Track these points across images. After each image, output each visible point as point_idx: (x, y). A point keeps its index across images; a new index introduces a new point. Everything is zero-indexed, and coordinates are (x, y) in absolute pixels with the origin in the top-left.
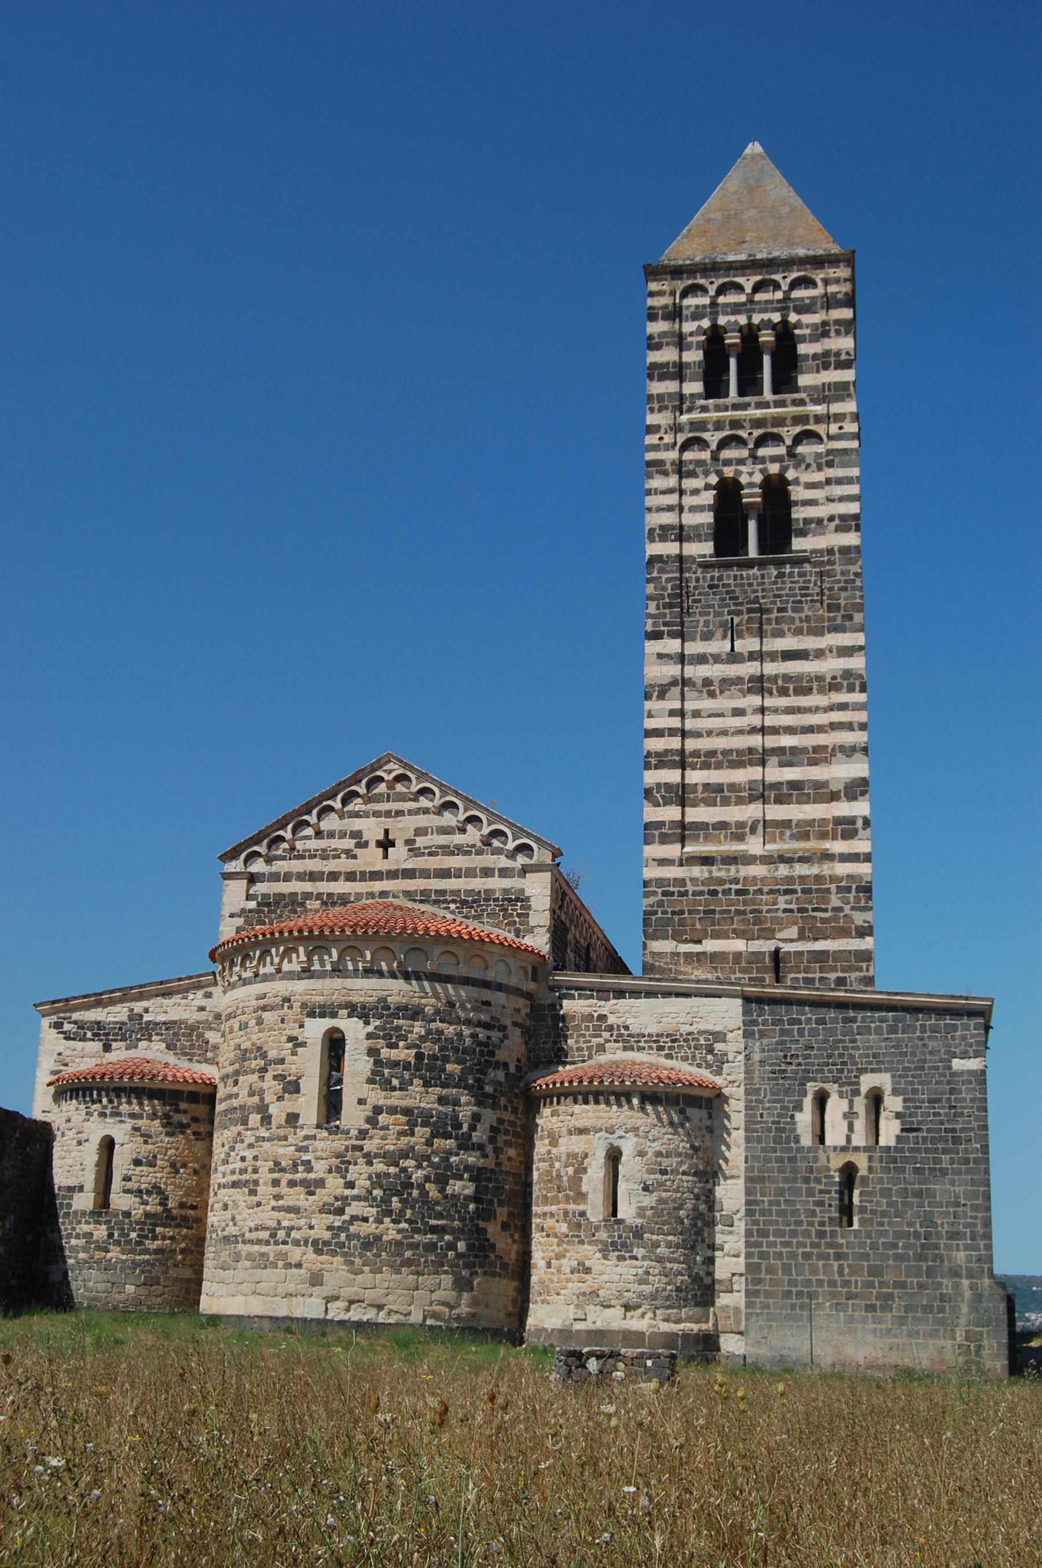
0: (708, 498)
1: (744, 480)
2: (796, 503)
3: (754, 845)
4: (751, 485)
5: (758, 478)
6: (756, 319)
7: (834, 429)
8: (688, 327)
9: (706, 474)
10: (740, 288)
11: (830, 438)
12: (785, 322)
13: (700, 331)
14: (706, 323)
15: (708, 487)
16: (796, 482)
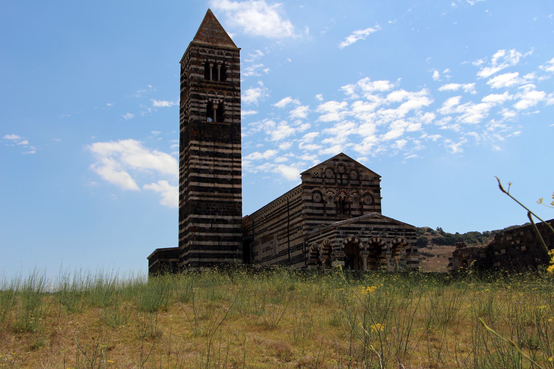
0: (205, 106)
1: (214, 102)
2: (226, 110)
3: (216, 193)
4: (216, 104)
5: (218, 102)
6: (218, 61)
7: (235, 93)
8: (202, 60)
9: (205, 100)
10: (214, 53)
11: (235, 95)
12: (224, 63)
13: (204, 62)
14: (205, 60)
15: (205, 103)
16: (226, 105)
